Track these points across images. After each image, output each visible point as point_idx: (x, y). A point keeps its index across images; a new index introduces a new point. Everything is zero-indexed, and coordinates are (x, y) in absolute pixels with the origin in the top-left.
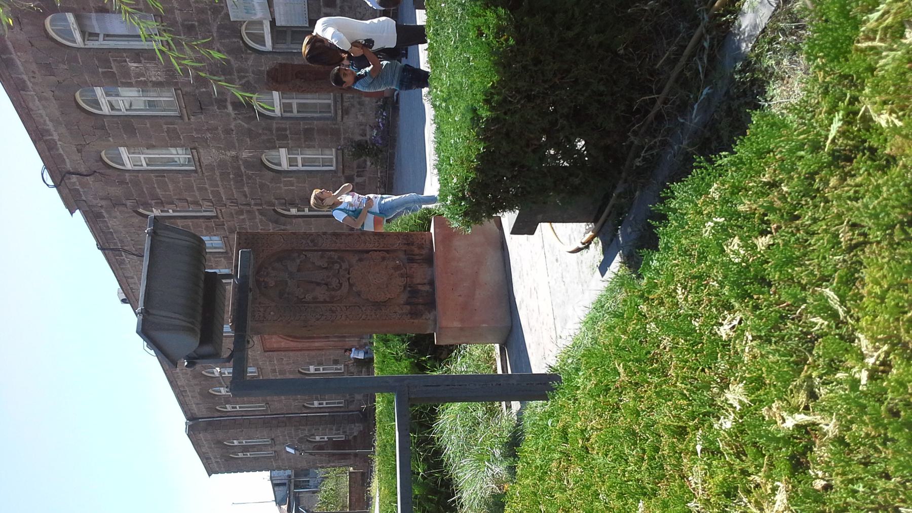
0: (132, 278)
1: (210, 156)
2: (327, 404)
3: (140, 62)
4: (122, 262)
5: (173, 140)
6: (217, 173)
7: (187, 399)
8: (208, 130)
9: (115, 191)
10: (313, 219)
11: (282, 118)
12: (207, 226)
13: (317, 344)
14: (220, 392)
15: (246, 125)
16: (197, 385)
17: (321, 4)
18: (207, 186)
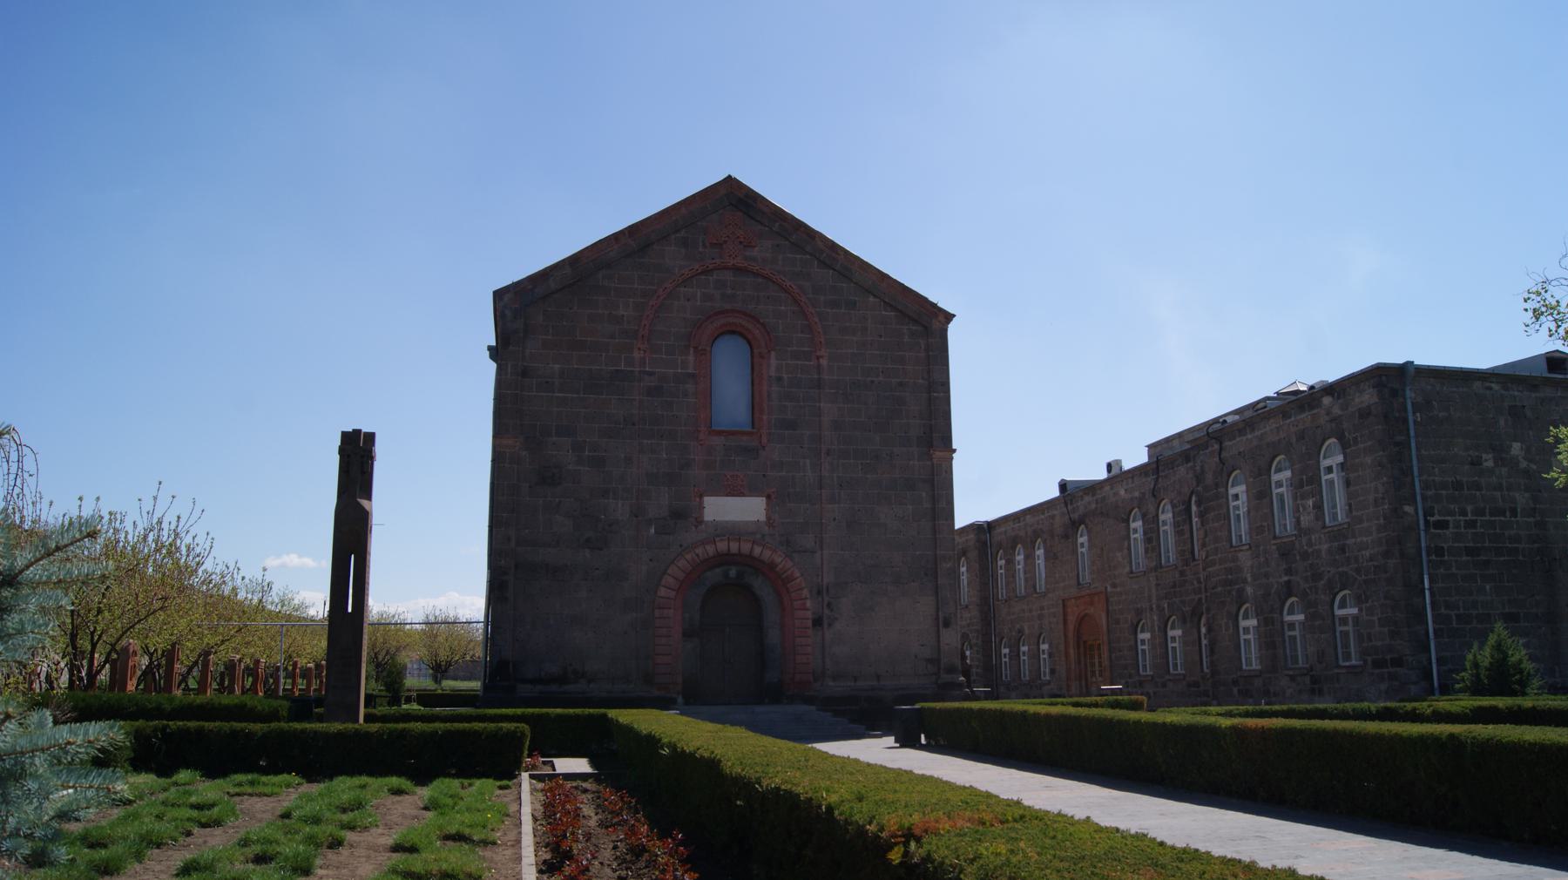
0: (1133, 482)
1: (1245, 559)
2: (1006, 662)
3: (1313, 509)
4: (1146, 474)
5: (1256, 530)
6: (1232, 565)
7: (1011, 523)
8: (1267, 559)
9: (1209, 478)
10: (1197, 648)
11: (1282, 622)
12: (1184, 551)
13: (1071, 651)
14: (1018, 554)
15: (1273, 591)
16: (1026, 533)
17: (1374, 657)
18: (1219, 556)
